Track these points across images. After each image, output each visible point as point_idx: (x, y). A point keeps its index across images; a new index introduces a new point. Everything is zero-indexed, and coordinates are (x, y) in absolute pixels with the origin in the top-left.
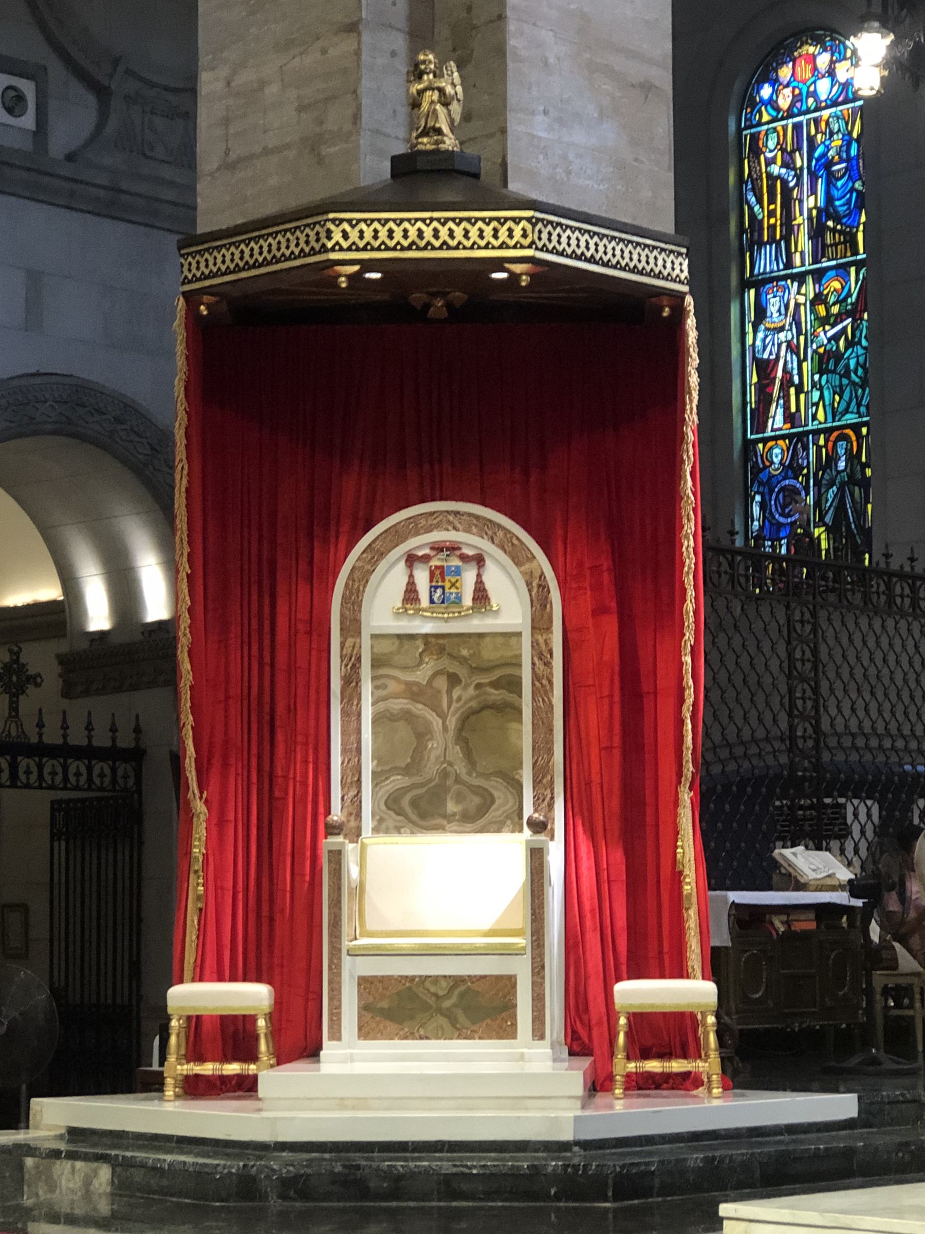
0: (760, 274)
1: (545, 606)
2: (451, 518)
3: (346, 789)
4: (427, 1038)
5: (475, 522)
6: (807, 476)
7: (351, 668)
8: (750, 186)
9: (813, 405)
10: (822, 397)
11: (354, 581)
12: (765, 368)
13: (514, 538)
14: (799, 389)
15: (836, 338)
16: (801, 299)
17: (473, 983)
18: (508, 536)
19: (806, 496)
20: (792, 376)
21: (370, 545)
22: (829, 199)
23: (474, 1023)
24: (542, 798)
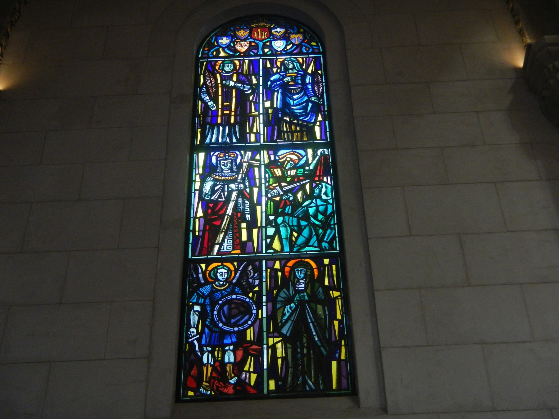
8: (204, 89)
9: (267, 237)
14: (252, 224)
15: (294, 192)
22: (285, 104)
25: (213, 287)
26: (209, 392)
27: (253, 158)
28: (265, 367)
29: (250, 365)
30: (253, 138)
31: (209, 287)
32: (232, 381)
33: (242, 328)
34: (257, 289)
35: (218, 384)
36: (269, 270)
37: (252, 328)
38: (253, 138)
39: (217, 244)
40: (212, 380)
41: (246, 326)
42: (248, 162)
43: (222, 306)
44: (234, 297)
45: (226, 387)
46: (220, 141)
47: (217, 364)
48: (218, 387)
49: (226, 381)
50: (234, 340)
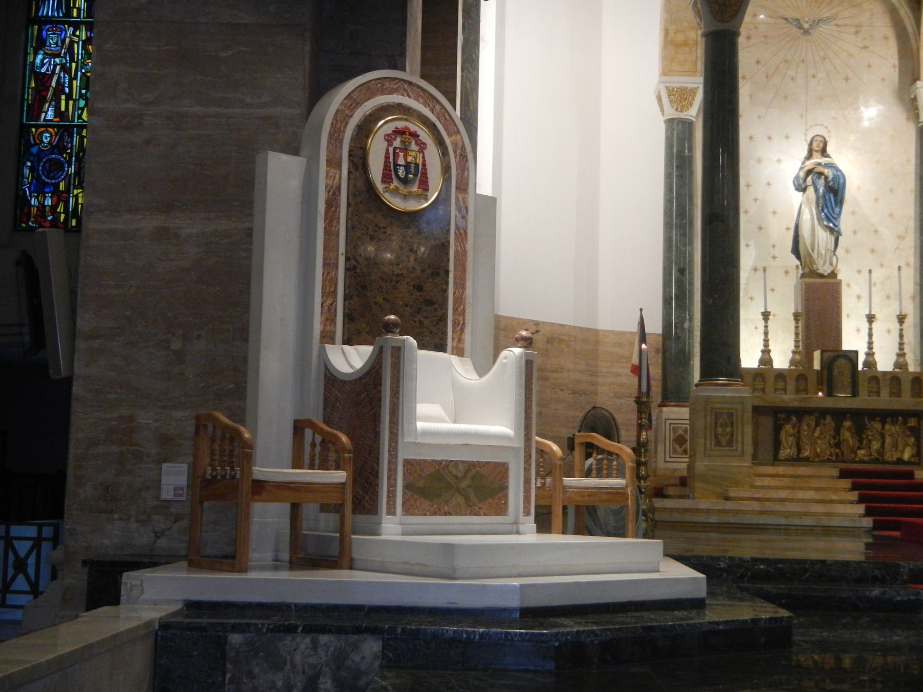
0: (42, 16)
1: (464, 172)
2: (406, 86)
3: (325, 297)
4: (450, 514)
5: (422, 94)
6: (70, 155)
7: (333, 194)
9: (79, 108)
10: (86, 105)
11: (337, 121)
12: (43, 80)
13: (446, 114)
14: (69, 97)
16: (76, 39)
17: (481, 467)
18: (443, 111)
19: (68, 168)
20: (64, 87)
21: (350, 94)
23: (480, 502)
24: (457, 323)
25: (39, 148)
26: (34, 225)
27: (74, 34)
28: (71, 210)
29: (60, 208)
30: (75, 14)
31: (37, 147)
32: (50, 218)
33: (34, 209)
34: (69, 151)
35: (40, 220)
36: (78, 137)
37: (64, 182)
38: (75, 14)
39: (44, 112)
40: (37, 217)
41: (60, 179)
42: (70, 37)
43: (45, 163)
44: (53, 156)
45: (45, 222)
46: (50, 14)
47: (40, 206)
48: (40, 222)
49: (45, 217)
50: (52, 189)
